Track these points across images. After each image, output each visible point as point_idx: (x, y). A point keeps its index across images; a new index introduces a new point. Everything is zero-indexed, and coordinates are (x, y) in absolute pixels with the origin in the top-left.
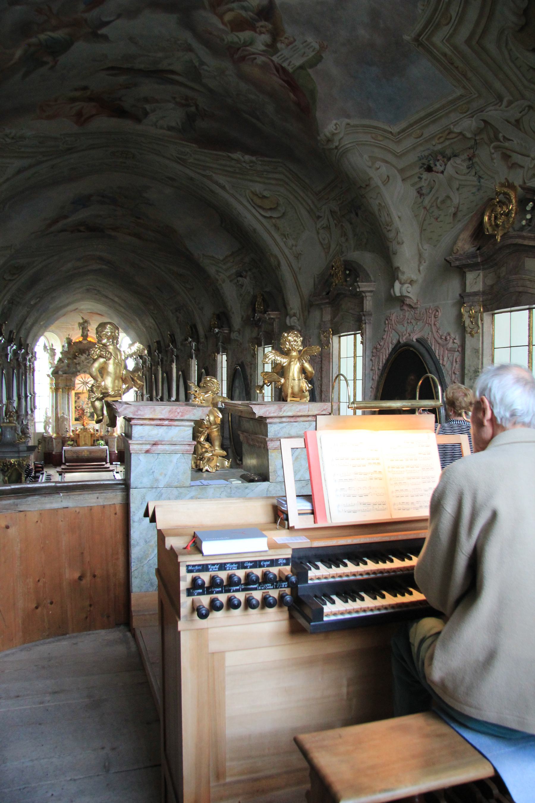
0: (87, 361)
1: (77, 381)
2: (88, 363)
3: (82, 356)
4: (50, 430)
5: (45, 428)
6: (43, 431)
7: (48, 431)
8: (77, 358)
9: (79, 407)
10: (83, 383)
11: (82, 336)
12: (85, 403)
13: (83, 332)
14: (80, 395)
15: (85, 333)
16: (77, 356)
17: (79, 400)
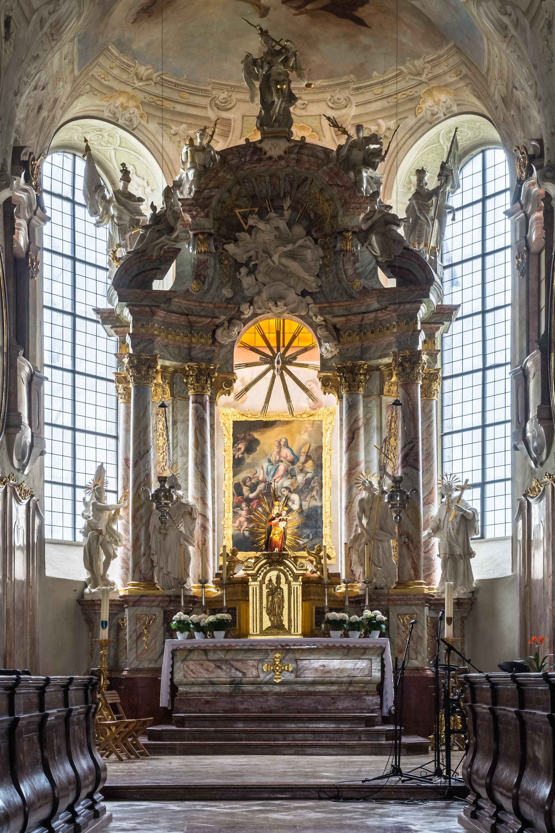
0: (290, 247)
3: (261, 225)
9: (253, 488)
10: (268, 360)
12: (282, 468)
13: (266, 105)
14: (256, 435)
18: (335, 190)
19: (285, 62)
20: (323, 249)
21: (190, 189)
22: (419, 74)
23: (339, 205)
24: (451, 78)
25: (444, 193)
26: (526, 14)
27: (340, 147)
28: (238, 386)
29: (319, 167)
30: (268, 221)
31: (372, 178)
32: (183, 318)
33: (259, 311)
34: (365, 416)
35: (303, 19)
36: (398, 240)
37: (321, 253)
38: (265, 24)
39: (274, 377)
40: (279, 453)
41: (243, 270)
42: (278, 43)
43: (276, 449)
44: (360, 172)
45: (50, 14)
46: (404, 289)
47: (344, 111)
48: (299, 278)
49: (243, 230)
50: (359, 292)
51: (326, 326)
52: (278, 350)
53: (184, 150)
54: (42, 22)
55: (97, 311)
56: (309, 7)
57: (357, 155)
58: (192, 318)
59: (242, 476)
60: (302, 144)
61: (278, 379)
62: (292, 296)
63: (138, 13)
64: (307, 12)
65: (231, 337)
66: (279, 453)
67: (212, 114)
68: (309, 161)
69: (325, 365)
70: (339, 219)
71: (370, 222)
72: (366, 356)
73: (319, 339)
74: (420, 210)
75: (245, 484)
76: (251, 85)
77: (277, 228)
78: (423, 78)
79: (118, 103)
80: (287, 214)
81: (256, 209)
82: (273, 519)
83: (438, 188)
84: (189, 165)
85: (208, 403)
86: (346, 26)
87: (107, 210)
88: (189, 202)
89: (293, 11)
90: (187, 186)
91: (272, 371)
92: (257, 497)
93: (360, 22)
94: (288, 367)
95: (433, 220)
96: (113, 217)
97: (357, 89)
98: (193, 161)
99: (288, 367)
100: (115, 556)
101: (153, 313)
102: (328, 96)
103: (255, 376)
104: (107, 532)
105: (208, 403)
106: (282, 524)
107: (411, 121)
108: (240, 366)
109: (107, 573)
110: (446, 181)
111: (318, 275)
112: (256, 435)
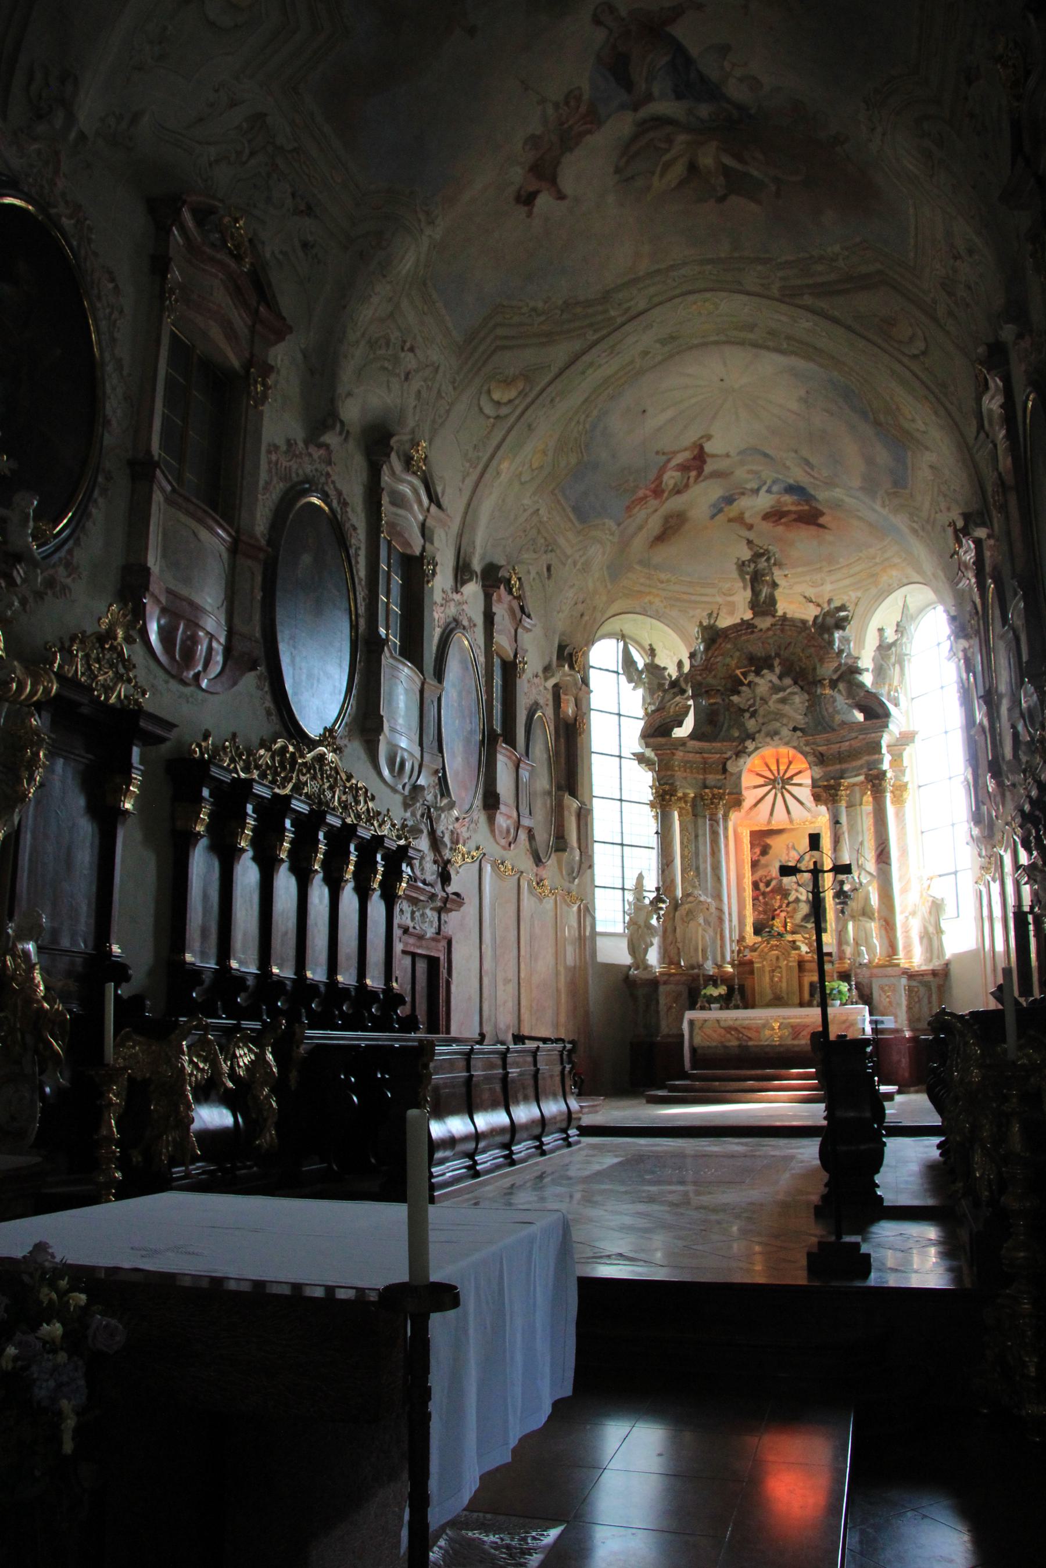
0: (781, 695)
1: (747, 780)
2: (783, 701)
3: (757, 680)
4: (653, 957)
5: (633, 949)
6: (626, 959)
7: (644, 960)
8: (744, 688)
9: (768, 884)
10: (773, 782)
11: (754, 605)
13: (755, 593)
14: (769, 841)
15: (765, 591)
16: (742, 684)
17: (767, 857)
18: (812, 650)
19: (768, 560)
20: (808, 694)
21: (701, 659)
22: (874, 558)
23: (816, 660)
24: (896, 560)
25: (901, 645)
26: (928, 521)
27: (816, 617)
28: (747, 804)
29: (800, 633)
30: (763, 676)
31: (843, 637)
32: (698, 755)
33: (760, 745)
34: (848, 823)
35: (780, 529)
36: (862, 685)
37: (806, 697)
38: (751, 535)
39: (776, 795)
40: (788, 854)
41: (747, 715)
42: (761, 548)
43: (785, 851)
44: (831, 635)
45: (580, 557)
46: (868, 722)
47: (821, 588)
48: (790, 718)
49: (743, 684)
50: (839, 725)
51: (814, 754)
52: (779, 774)
53: (696, 629)
54: (575, 564)
55: (634, 754)
56: (783, 520)
57: (830, 621)
58: (706, 755)
59: (761, 873)
60: (784, 618)
61: (779, 795)
62: (785, 732)
63: (653, 542)
64: (781, 524)
65: (738, 767)
66: (788, 854)
67: (719, 599)
68: (790, 630)
69: (814, 785)
70: (818, 670)
71: (839, 673)
72: (846, 775)
73: (809, 764)
74: (883, 659)
75: (761, 881)
76: (744, 580)
77: (771, 681)
78: (877, 560)
79: (646, 601)
80: (778, 670)
81: (753, 668)
82: (776, 910)
83: (896, 640)
84: (700, 640)
85: (721, 820)
86: (813, 529)
87: (640, 678)
88: (700, 668)
89: (772, 525)
90: (699, 656)
91: (774, 791)
92: (772, 891)
93: (822, 526)
94: (787, 787)
95: (894, 665)
96: (644, 683)
97: (830, 571)
98: (703, 637)
99: (787, 787)
100: (652, 944)
101: (673, 754)
102: (808, 578)
103: (761, 795)
104: (645, 926)
105: (721, 820)
106: (783, 914)
107: (874, 591)
108: (748, 788)
109: (647, 957)
110: (902, 636)
111: (805, 714)
112: (769, 841)
